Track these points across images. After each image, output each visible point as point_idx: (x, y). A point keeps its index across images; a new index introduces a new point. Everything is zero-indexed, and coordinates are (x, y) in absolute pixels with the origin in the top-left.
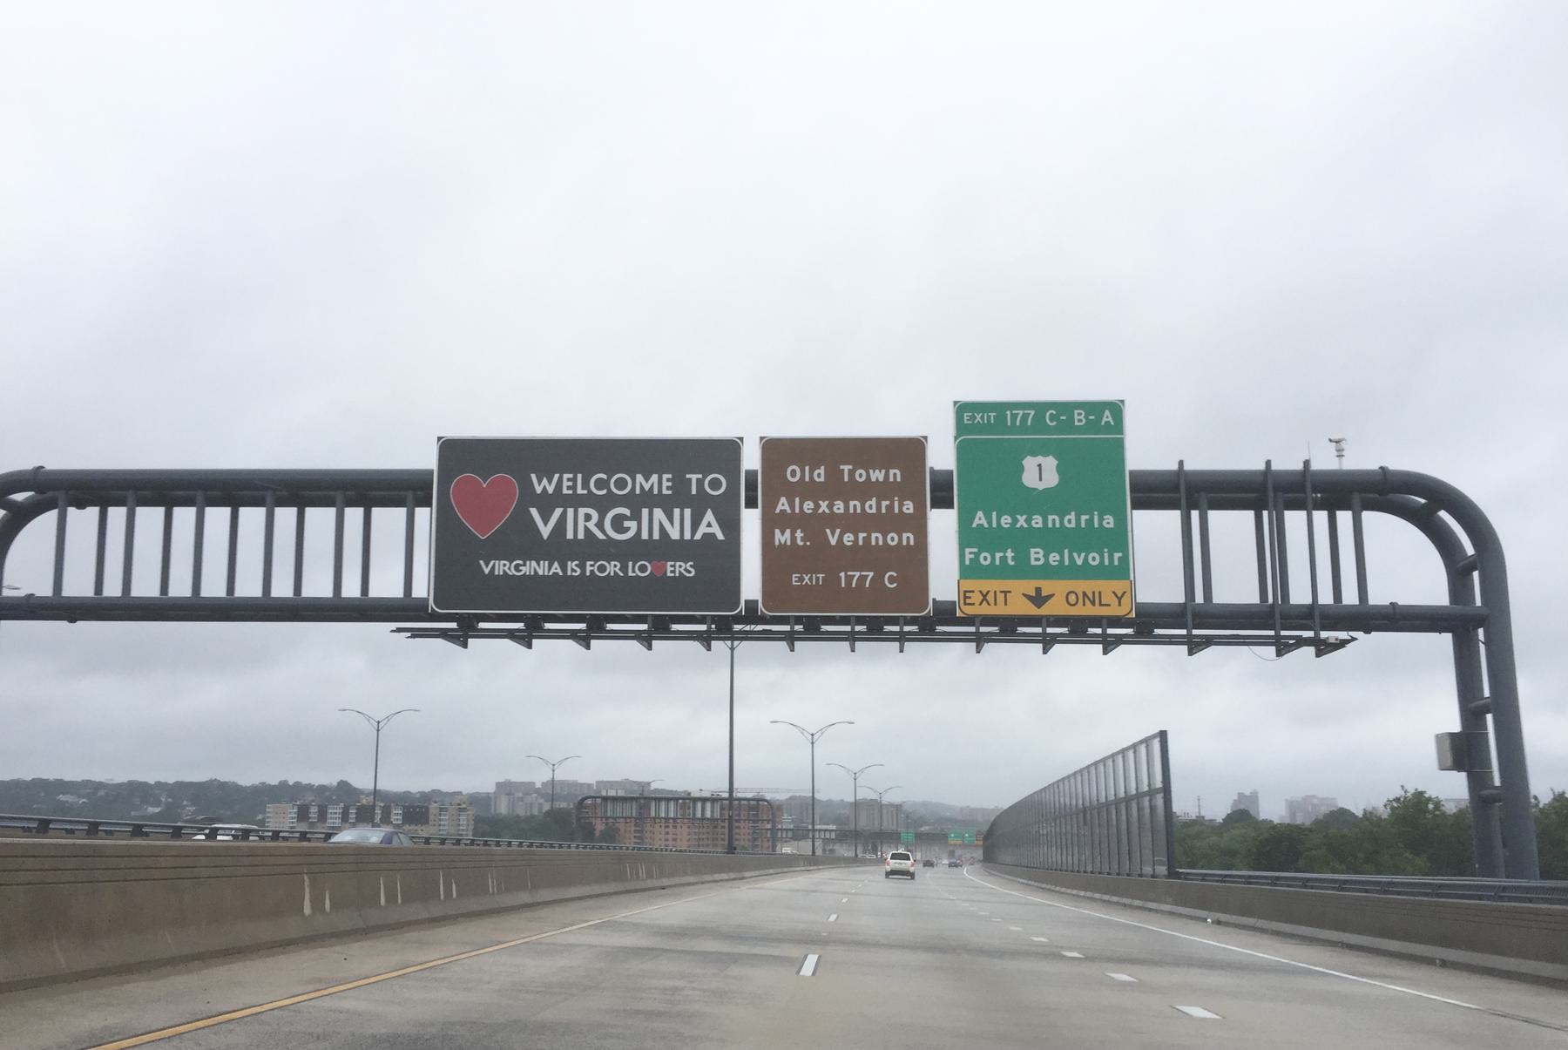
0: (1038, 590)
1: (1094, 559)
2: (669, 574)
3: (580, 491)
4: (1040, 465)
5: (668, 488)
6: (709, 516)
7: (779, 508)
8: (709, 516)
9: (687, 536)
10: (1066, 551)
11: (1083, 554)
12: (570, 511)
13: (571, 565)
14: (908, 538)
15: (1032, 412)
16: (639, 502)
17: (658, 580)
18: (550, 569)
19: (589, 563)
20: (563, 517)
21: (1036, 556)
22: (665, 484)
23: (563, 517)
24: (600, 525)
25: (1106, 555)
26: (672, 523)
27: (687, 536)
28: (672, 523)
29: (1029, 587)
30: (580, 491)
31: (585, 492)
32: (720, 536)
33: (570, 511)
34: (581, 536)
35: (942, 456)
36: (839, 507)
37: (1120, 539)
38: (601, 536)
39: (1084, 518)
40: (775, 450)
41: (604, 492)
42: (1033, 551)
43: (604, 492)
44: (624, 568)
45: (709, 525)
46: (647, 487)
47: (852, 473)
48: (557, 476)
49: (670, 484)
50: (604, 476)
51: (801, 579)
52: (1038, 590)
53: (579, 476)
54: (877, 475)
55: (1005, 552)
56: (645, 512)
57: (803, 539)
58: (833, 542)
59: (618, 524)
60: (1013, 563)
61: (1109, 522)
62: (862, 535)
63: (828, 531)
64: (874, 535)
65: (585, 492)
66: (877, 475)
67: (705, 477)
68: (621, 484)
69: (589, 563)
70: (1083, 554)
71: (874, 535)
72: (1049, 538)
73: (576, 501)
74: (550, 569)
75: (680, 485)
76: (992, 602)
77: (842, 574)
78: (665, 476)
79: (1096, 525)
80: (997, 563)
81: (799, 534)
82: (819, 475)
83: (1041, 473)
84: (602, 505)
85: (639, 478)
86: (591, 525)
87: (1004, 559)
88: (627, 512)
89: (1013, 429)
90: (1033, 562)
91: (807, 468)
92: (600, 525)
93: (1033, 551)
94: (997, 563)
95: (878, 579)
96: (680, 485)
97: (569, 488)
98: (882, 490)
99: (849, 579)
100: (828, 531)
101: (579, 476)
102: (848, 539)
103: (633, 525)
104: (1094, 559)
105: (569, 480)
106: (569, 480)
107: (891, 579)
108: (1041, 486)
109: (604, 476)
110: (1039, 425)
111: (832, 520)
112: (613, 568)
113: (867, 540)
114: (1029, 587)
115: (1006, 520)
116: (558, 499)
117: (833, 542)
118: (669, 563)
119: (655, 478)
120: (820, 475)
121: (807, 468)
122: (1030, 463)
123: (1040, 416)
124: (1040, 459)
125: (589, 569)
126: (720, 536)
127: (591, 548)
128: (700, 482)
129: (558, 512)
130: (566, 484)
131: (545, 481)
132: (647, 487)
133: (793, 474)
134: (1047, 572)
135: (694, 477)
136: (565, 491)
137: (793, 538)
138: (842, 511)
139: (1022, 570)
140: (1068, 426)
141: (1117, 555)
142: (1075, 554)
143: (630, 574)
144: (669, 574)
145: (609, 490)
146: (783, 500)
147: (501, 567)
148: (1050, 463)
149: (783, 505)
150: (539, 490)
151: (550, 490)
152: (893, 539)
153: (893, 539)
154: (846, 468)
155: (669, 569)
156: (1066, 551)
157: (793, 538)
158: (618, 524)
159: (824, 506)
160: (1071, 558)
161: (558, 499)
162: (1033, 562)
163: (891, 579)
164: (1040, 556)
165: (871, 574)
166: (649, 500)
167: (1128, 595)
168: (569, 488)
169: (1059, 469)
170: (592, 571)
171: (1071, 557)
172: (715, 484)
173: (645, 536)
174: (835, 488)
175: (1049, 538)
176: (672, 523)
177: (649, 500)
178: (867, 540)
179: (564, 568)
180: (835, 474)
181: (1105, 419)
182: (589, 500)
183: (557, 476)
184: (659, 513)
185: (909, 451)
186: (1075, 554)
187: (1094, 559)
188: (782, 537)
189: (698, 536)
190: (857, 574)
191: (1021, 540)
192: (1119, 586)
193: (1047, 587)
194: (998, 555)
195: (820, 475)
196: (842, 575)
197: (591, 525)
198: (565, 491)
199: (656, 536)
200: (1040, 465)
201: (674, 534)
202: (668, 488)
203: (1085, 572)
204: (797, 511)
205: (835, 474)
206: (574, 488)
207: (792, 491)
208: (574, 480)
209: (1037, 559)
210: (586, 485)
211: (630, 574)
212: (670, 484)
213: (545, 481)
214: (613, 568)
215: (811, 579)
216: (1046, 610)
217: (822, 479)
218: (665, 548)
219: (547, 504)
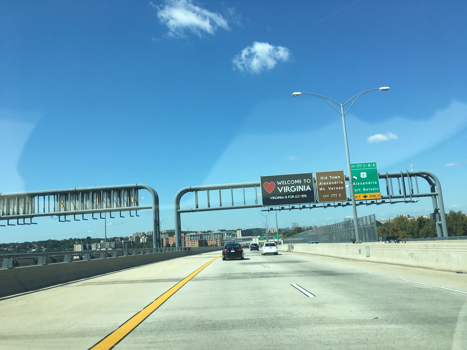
0: (365, 195)
1: (374, 189)
2: (302, 197)
3: (286, 184)
4: (363, 174)
5: (301, 182)
6: (308, 186)
7: (320, 184)
8: (308, 186)
9: (305, 190)
10: (369, 188)
11: (372, 189)
12: (284, 187)
13: (286, 197)
14: (342, 188)
15: (361, 165)
16: (296, 185)
17: (301, 198)
18: (282, 197)
19: (288, 196)
20: (283, 188)
21: (364, 189)
22: (300, 181)
23: (283, 188)
24: (290, 189)
25: (376, 189)
26: (300, 189)
27: (305, 190)
28: (302, 188)
29: (363, 195)
30: (286, 184)
31: (286, 184)
32: (310, 190)
33: (284, 187)
34: (287, 191)
35: (347, 174)
36: (330, 183)
37: (377, 186)
38: (290, 191)
39: (372, 182)
40: (319, 175)
41: (290, 184)
42: (363, 189)
43: (290, 184)
44: (295, 197)
45: (308, 188)
46: (297, 182)
47: (332, 177)
48: (281, 181)
49: (301, 181)
50: (290, 181)
51: (325, 196)
52: (365, 195)
53: (285, 181)
54: (336, 177)
55: (359, 189)
56: (297, 186)
57: (324, 189)
58: (330, 189)
59: (293, 189)
60: (360, 191)
61: (376, 183)
62: (334, 188)
63: (329, 188)
64: (336, 188)
65: (286, 184)
66: (336, 177)
67: (307, 180)
68: (292, 182)
69: (288, 196)
70: (372, 189)
71: (336, 188)
72: (366, 186)
73: (285, 186)
74: (282, 197)
75: (303, 181)
76: (357, 198)
77: (332, 195)
78: (300, 180)
79: (374, 183)
80: (358, 191)
81: (324, 188)
82: (326, 178)
83: (364, 175)
84: (290, 186)
85: (295, 181)
86: (288, 189)
87: (359, 190)
88: (294, 187)
89: (358, 168)
90: (364, 191)
91: (324, 177)
92: (290, 189)
93: (363, 189)
94: (358, 191)
95: (338, 195)
96: (303, 181)
97: (284, 183)
98: (337, 180)
99: (333, 196)
100: (329, 188)
101: (285, 181)
102: (332, 189)
103: (295, 189)
104: (374, 189)
105: (283, 182)
106: (283, 182)
107: (340, 195)
108: (364, 177)
109: (290, 181)
110: (362, 167)
111: (329, 186)
112: (293, 197)
113: (335, 189)
114: (363, 195)
115: (359, 184)
116: (282, 185)
117: (330, 189)
118: (302, 195)
119: (298, 181)
120: (326, 178)
121: (324, 177)
122: (362, 174)
123: (362, 166)
124: (363, 173)
125: (289, 197)
126: (310, 190)
127: (289, 194)
128: (306, 181)
129: (282, 187)
130: (283, 183)
131: (279, 182)
132: (297, 182)
133: (322, 178)
134: (366, 192)
135: (305, 180)
136: (283, 184)
137: (323, 189)
138: (331, 184)
139: (362, 192)
140: (368, 167)
141: (378, 188)
142: (371, 189)
143: (296, 197)
144: (302, 197)
145: (291, 183)
146: (320, 183)
147: (274, 198)
148: (365, 173)
149: (320, 184)
150: (279, 184)
151: (281, 184)
152: (340, 188)
153: (340, 188)
154: (331, 177)
155: (302, 196)
156: (369, 188)
157: (323, 189)
158: (293, 189)
159: (327, 183)
160: (370, 189)
161: (282, 185)
162: (364, 191)
163: (340, 195)
164: (365, 189)
165: (337, 194)
166: (298, 184)
167: (380, 195)
168: (284, 183)
169: (366, 174)
170: (289, 197)
171: (370, 189)
172: (309, 181)
173: (298, 191)
174: (329, 180)
175: (366, 186)
176: (302, 188)
177: (298, 184)
178: (335, 189)
179: (284, 197)
180: (328, 178)
181: (373, 165)
182: (287, 185)
183: (281, 181)
184: (299, 187)
185: (340, 173)
186: (371, 189)
187: (374, 189)
188: (321, 189)
189: (307, 190)
190: (334, 195)
191: (362, 187)
192: (379, 193)
193: (367, 194)
194: (358, 190)
195: (326, 178)
196: (332, 195)
197: (288, 189)
198: (283, 184)
199: (299, 191)
200: (363, 174)
201: (303, 190)
202: (301, 182)
203: (373, 192)
204: (323, 184)
205: (328, 178)
206: (284, 183)
207: (322, 181)
208: (285, 182)
209: (364, 190)
210: (286, 183)
211: (296, 197)
212: (301, 181)
213: (279, 182)
214: (293, 197)
215: (326, 196)
216: (367, 198)
217: (327, 179)
218: (301, 193)
219: (280, 186)
